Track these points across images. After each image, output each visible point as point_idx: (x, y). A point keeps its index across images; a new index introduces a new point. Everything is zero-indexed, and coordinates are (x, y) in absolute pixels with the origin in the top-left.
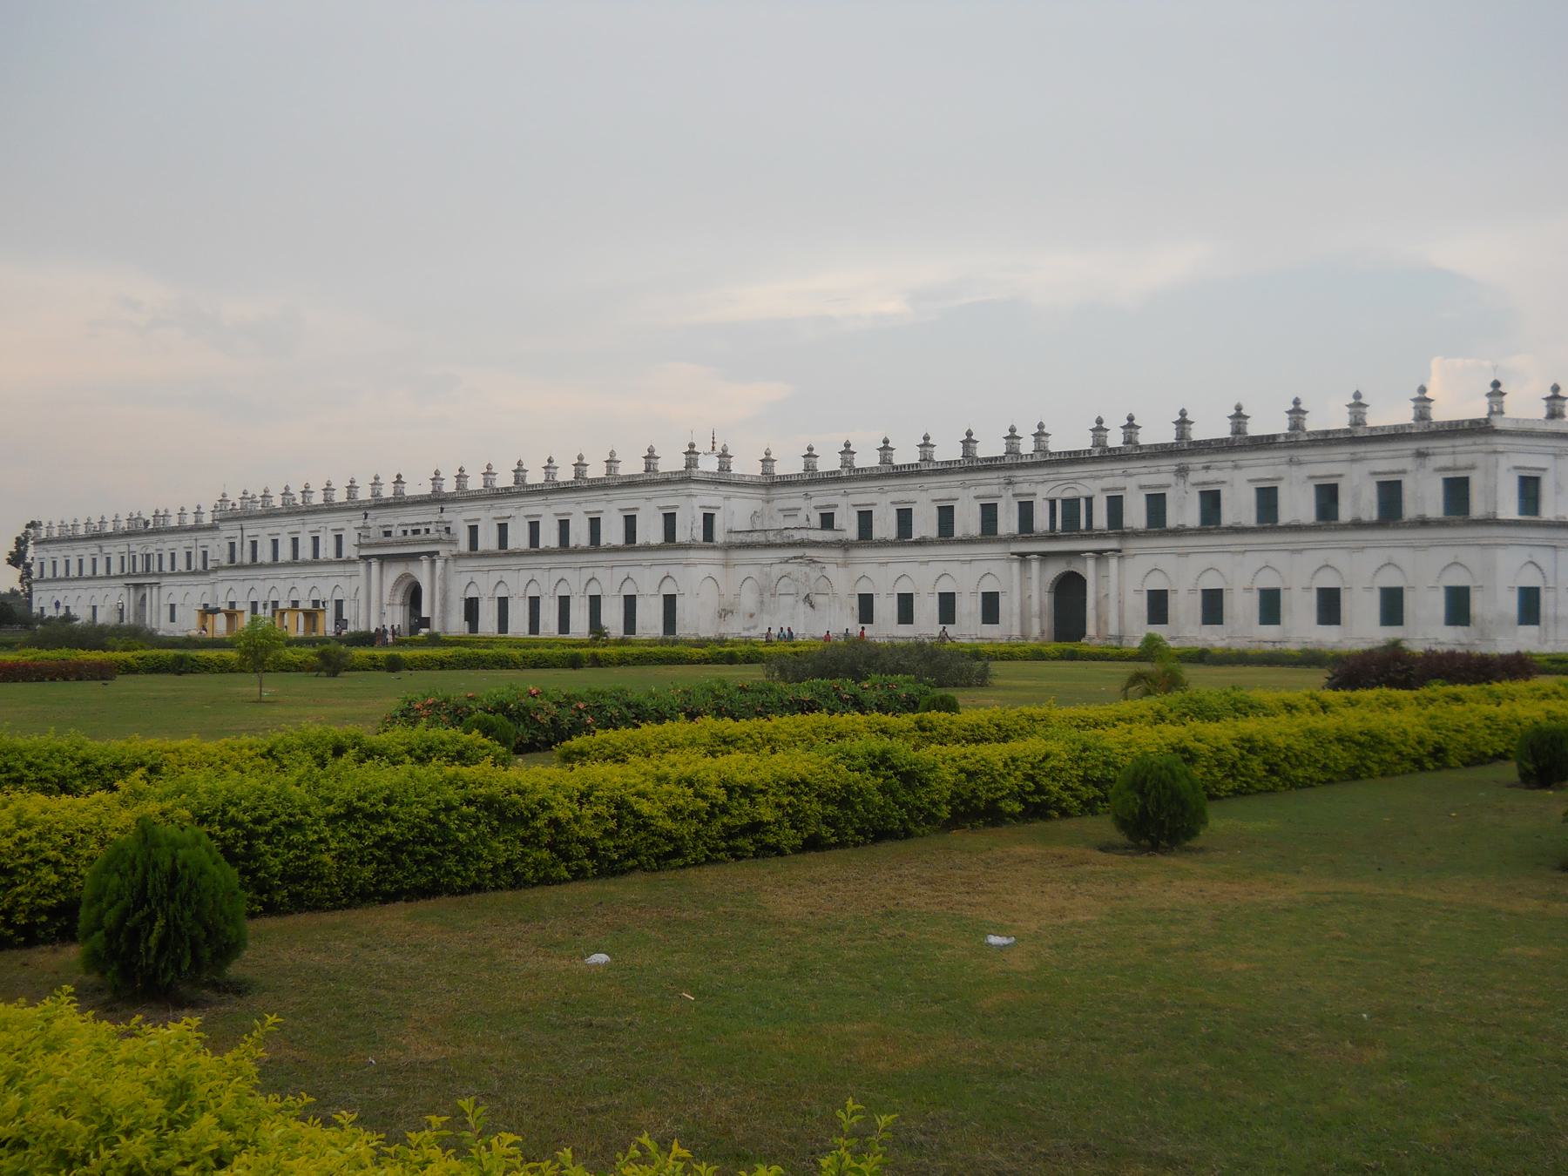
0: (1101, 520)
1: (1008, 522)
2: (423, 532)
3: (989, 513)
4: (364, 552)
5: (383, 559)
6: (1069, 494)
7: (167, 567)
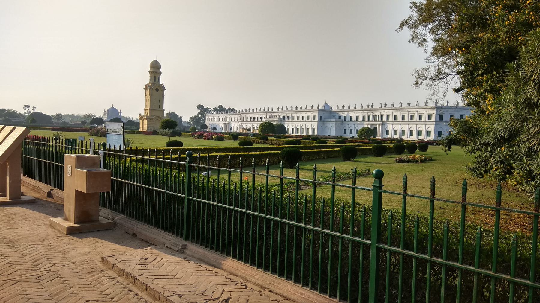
1: (366, 119)
3: (364, 117)
7: (230, 121)
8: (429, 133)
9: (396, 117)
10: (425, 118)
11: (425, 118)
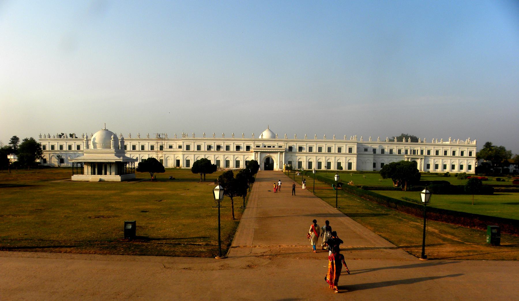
0: (419, 153)
2: (272, 147)
4: (255, 150)
5: (261, 152)
6: (414, 149)
8: (470, 167)
9: (437, 152)
10: (466, 154)
11: (466, 154)
